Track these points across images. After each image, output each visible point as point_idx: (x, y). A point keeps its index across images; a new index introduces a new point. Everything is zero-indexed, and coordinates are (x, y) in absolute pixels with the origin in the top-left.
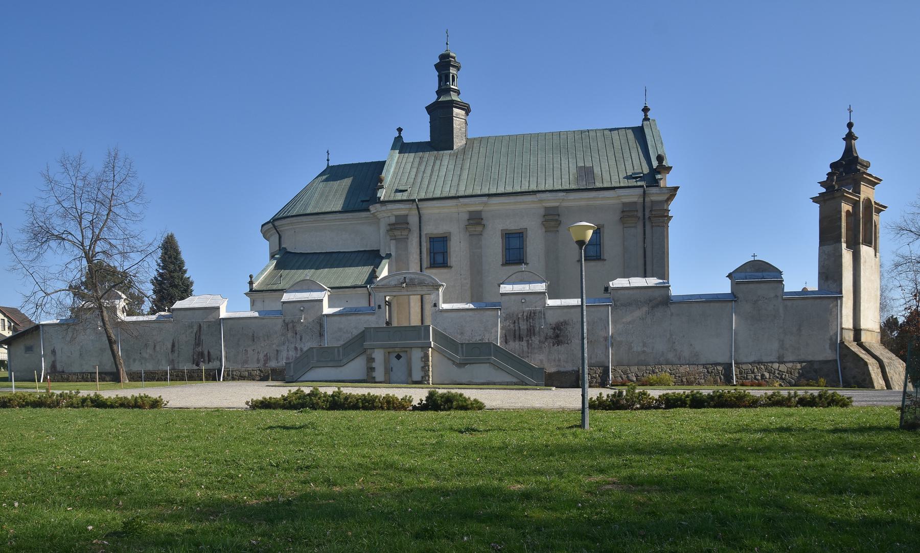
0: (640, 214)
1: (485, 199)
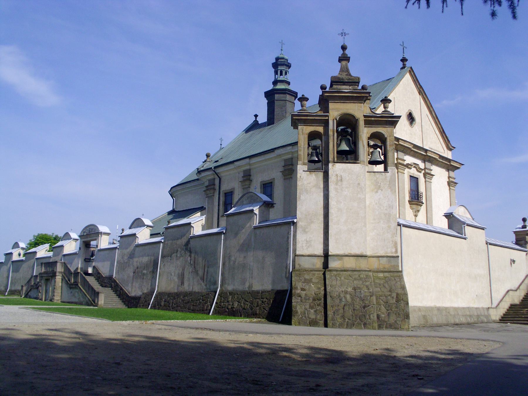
1: (247, 160)
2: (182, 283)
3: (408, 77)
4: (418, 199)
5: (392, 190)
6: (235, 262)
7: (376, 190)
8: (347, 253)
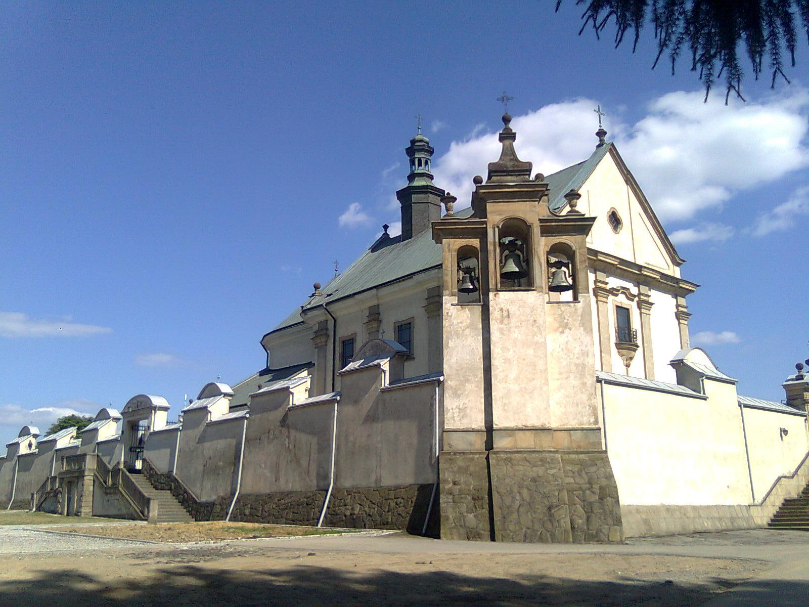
1: (374, 291)
3: (608, 159)
4: (631, 341)
5: (585, 329)
7: (561, 329)
8: (520, 426)
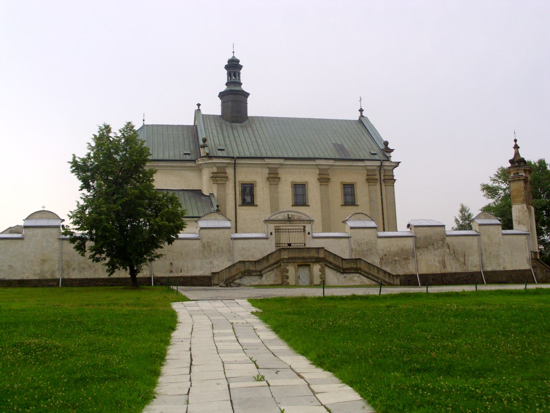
0: (378, 177)
2: (444, 267)
6: (490, 254)
